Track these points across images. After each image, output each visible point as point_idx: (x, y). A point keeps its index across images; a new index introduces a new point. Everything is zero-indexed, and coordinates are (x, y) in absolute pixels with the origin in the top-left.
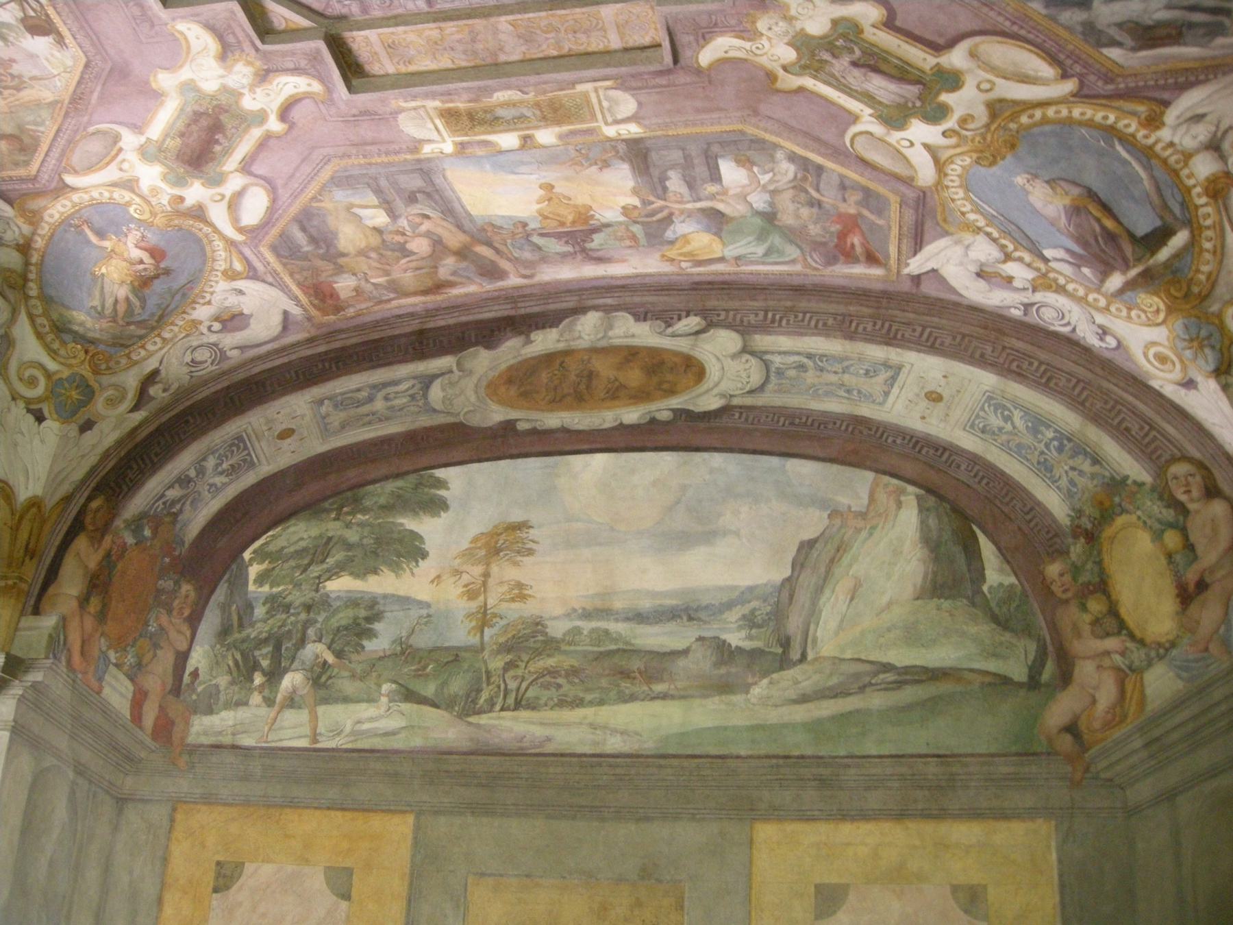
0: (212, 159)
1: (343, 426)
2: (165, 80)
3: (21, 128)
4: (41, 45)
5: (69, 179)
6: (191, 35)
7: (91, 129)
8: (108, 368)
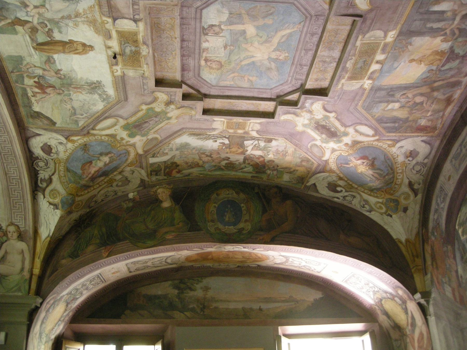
1: (460, 165)
4: (274, 143)
5: (324, 159)
8: (394, 191)
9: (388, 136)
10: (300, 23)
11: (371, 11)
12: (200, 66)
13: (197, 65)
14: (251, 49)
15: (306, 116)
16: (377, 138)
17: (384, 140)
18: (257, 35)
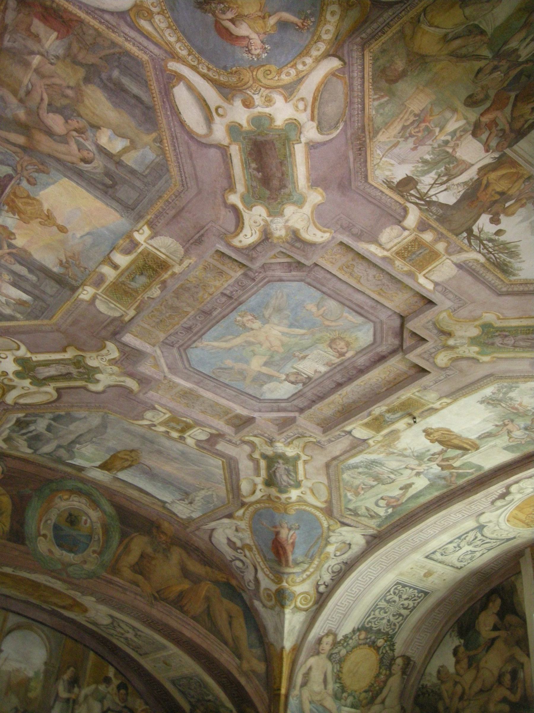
0: (250, 154)
2: (315, 197)
3: (391, 94)
4: (400, 173)
5: (334, 63)
6: (319, 234)
7: (341, 126)
9: (144, 49)
10: (196, 347)
11: (105, 339)
12: (357, 353)
13: (360, 355)
14: (277, 343)
15: (280, 225)
16: (173, 66)
17: (156, 44)
18: (255, 355)
